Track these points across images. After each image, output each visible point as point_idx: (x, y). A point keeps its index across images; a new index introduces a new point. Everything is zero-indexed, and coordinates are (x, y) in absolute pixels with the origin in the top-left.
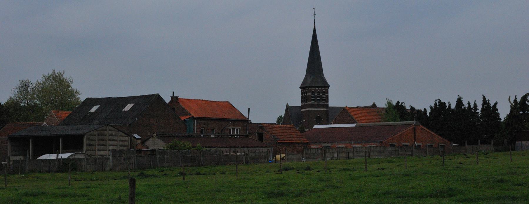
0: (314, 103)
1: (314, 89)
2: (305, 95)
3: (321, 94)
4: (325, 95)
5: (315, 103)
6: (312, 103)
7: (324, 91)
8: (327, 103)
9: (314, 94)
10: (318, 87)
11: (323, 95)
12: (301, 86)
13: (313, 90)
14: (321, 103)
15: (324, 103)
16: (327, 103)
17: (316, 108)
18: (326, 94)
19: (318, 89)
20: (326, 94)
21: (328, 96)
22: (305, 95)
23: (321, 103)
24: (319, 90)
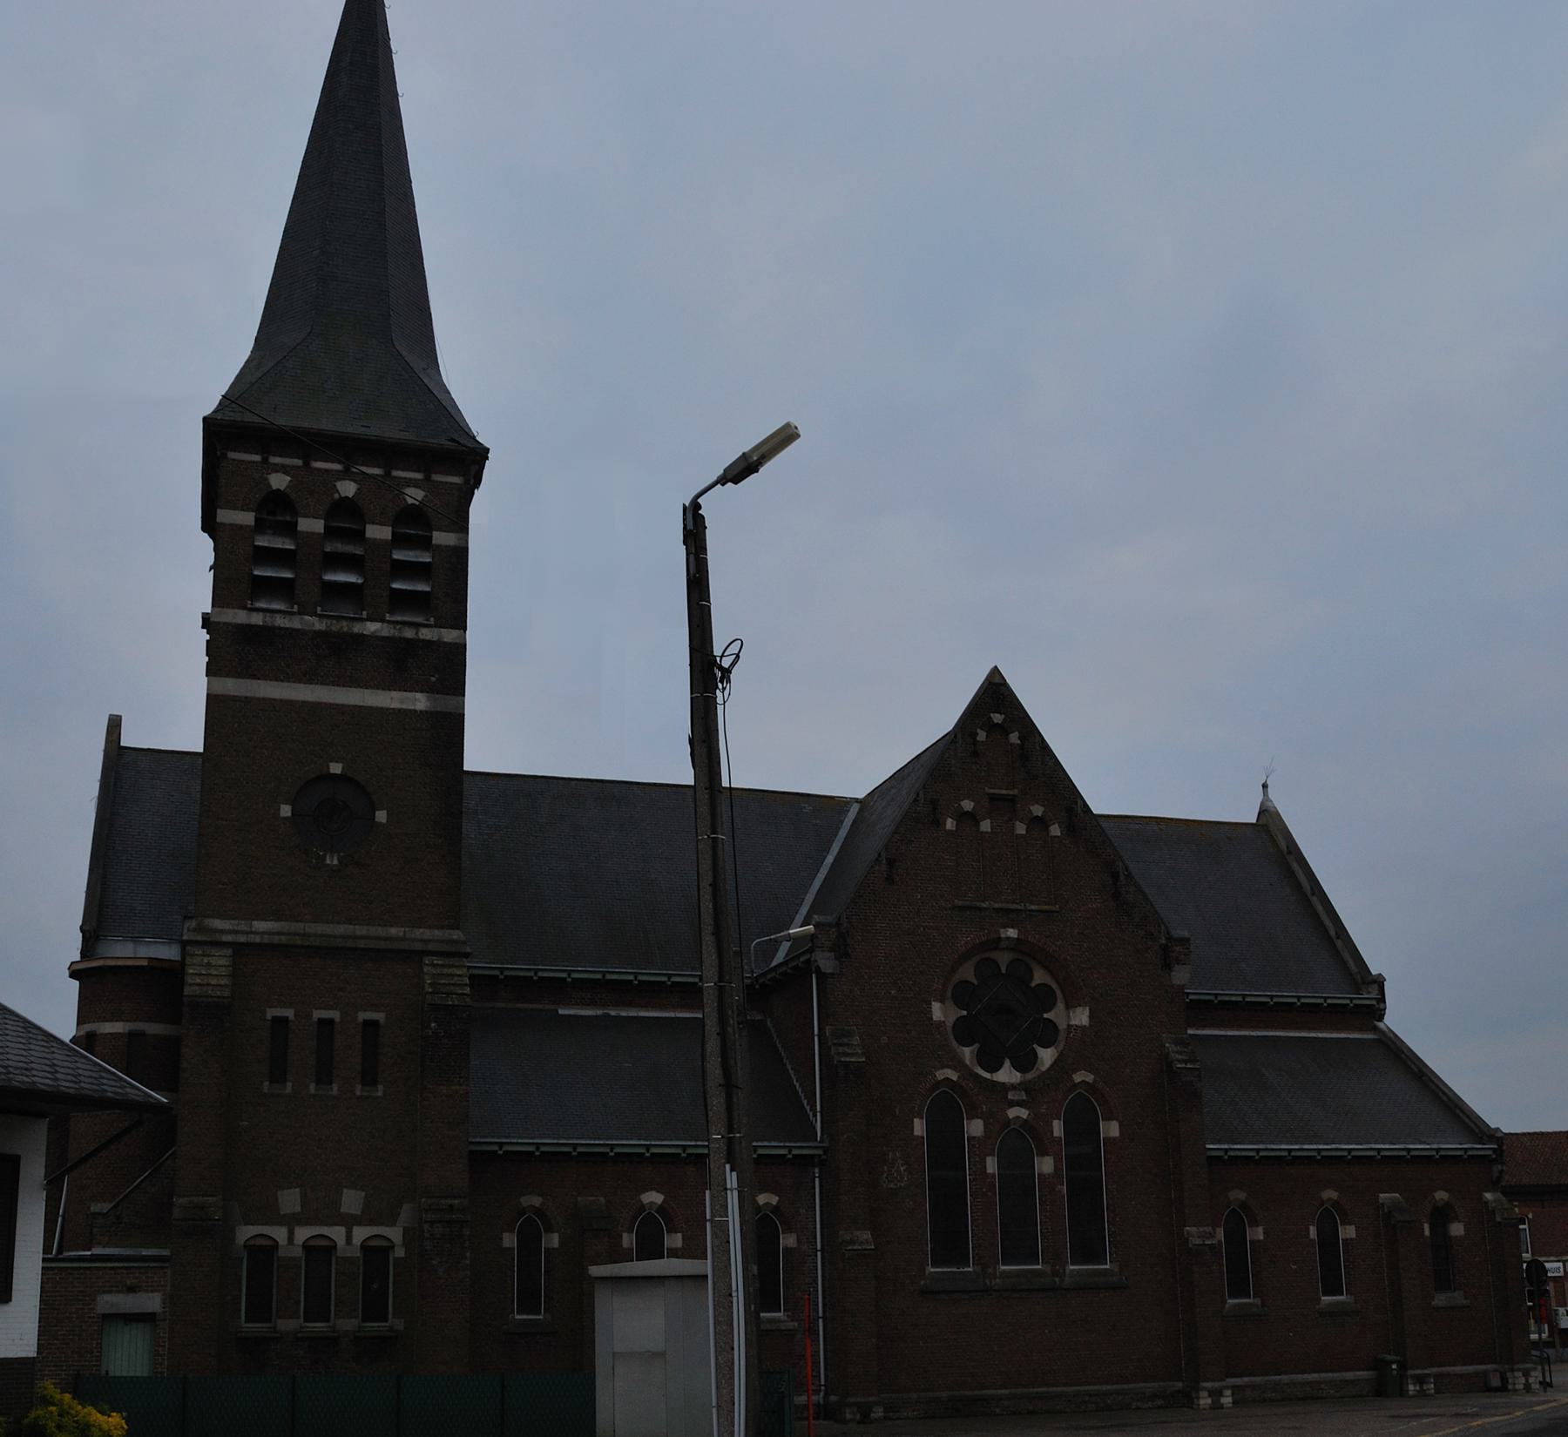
0: (280, 621)
1: (284, 469)
2: (529, 1240)
3: (379, 532)
4: (425, 543)
5: (296, 623)
6: (257, 619)
7: (414, 495)
8: (449, 635)
9: (290, 529)
10: (349, 449)
11: (399, 541)
12: (215, 411)
13: (279, 481)
14: (372, 627)
15: (409, 633)
16: (449, 635)
17: (309, 678)
18: (441, 538)
19: (346, 474)
20: (441, 538)
21: (460, 556)
22: (529, 1240)
23: (372, 627)
24: (348, 489)
